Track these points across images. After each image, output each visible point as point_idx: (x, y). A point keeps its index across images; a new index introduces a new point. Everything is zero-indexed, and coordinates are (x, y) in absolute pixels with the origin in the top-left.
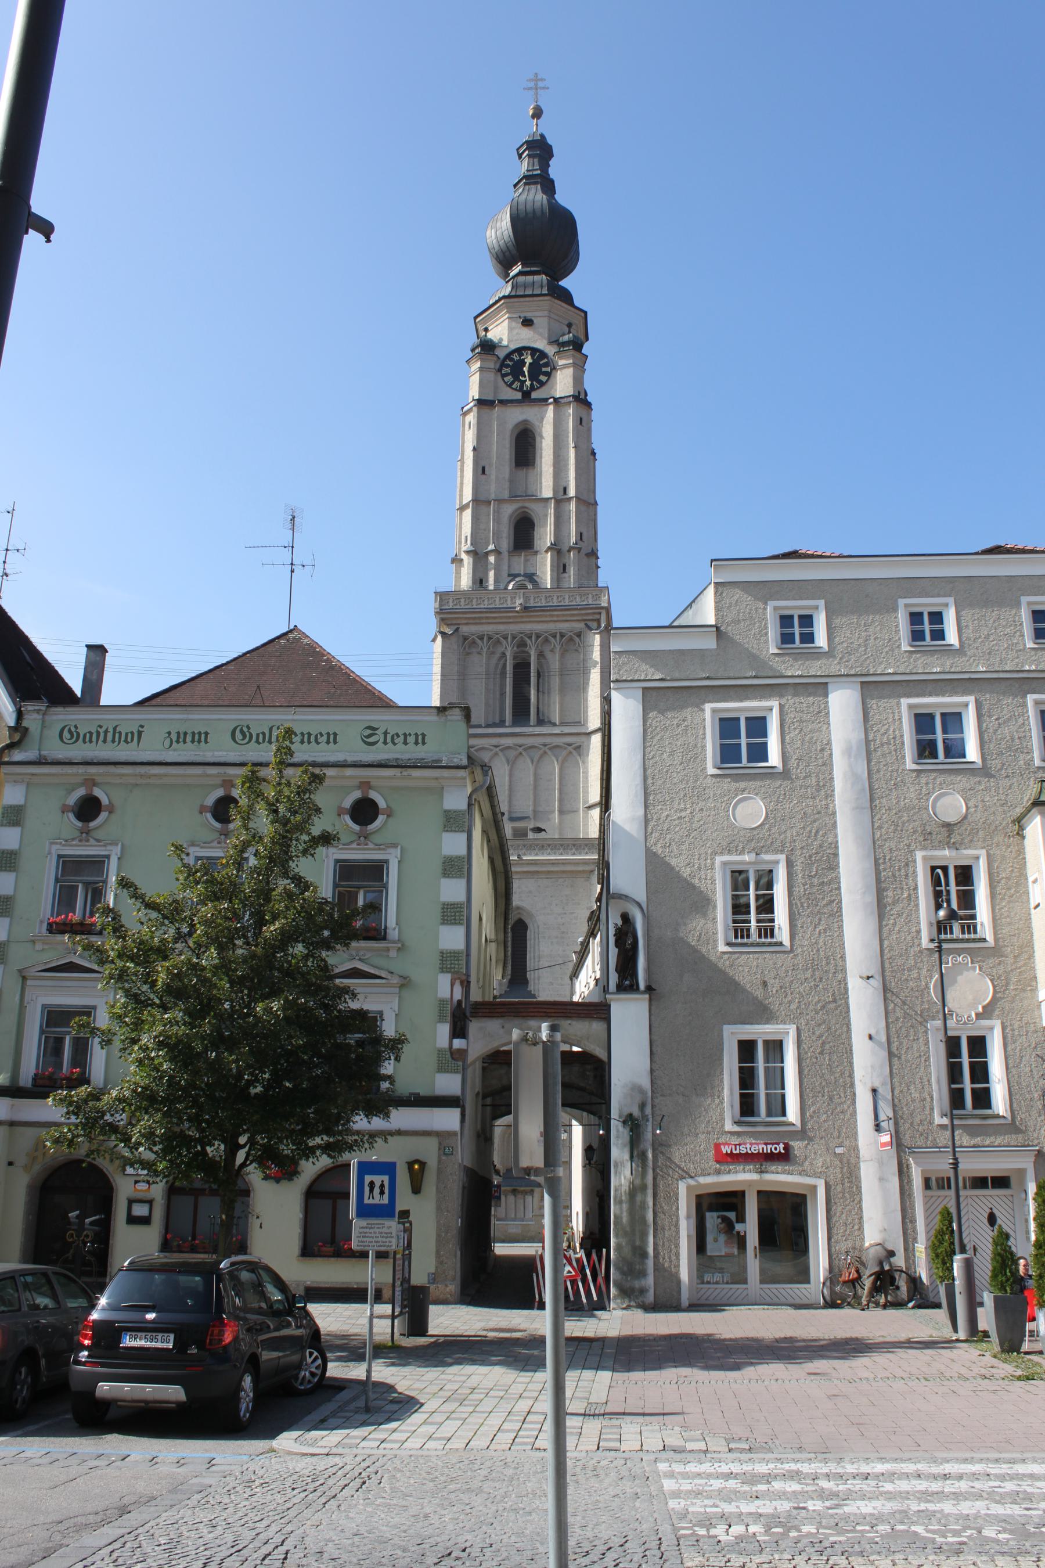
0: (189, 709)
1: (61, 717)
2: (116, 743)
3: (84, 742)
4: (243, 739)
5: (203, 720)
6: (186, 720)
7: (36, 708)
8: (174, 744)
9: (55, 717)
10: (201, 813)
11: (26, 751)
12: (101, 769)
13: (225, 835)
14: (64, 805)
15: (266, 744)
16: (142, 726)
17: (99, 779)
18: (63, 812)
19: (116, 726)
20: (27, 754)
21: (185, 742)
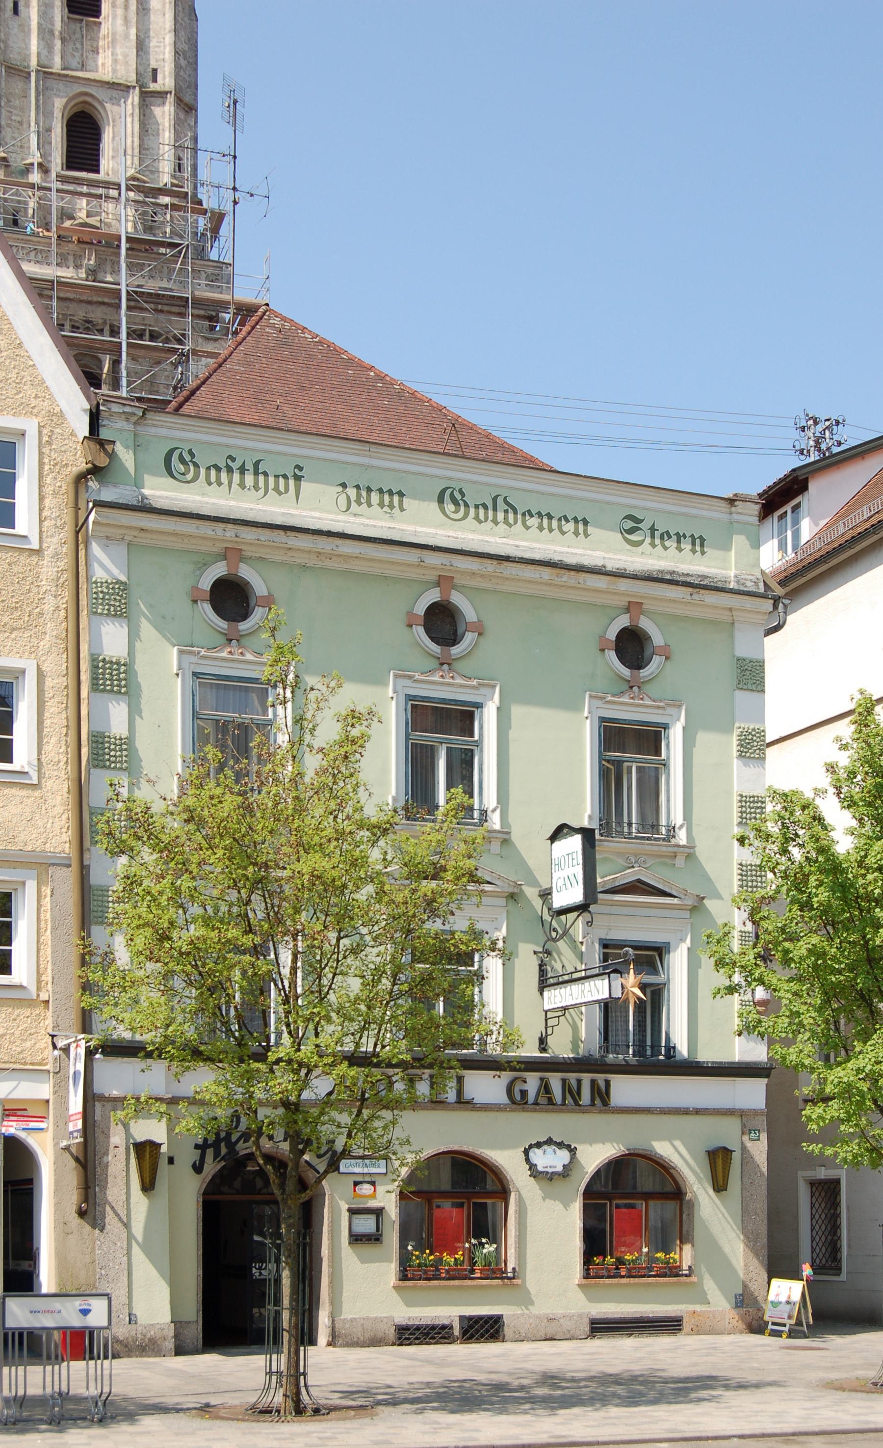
0: (374, 448)
1: (163, 432)
2: (262, 491)
3: (210, 484)
4: (456, 512)
5: (393, 470)
6: (367, 467)
7: (128, 409)
8: (353, 504)
9: (153, 431)
10: (410, 626)
11: (115, 485)
12: (265, 534)
13: (449, 664)
14: (195, 588)
15: (490, 524)
16: (301, 469)
17: (248, 551)
18: (195, 601)
19: (258, 462)
20: (118, 490)
21: (369, 505)
